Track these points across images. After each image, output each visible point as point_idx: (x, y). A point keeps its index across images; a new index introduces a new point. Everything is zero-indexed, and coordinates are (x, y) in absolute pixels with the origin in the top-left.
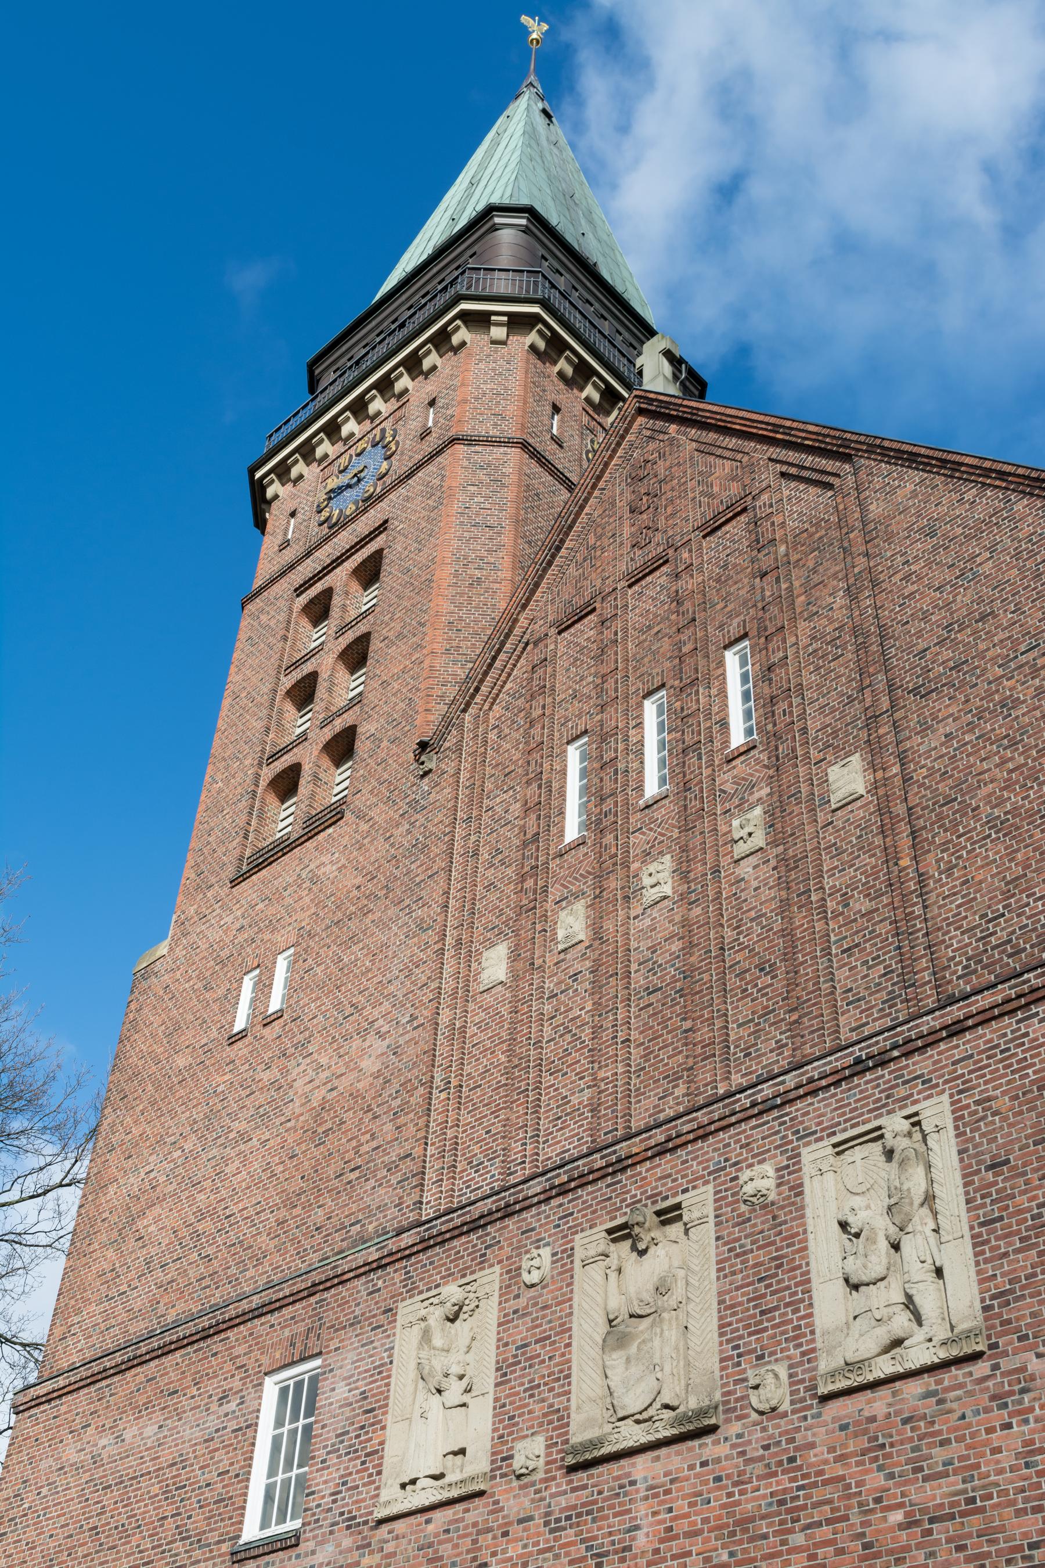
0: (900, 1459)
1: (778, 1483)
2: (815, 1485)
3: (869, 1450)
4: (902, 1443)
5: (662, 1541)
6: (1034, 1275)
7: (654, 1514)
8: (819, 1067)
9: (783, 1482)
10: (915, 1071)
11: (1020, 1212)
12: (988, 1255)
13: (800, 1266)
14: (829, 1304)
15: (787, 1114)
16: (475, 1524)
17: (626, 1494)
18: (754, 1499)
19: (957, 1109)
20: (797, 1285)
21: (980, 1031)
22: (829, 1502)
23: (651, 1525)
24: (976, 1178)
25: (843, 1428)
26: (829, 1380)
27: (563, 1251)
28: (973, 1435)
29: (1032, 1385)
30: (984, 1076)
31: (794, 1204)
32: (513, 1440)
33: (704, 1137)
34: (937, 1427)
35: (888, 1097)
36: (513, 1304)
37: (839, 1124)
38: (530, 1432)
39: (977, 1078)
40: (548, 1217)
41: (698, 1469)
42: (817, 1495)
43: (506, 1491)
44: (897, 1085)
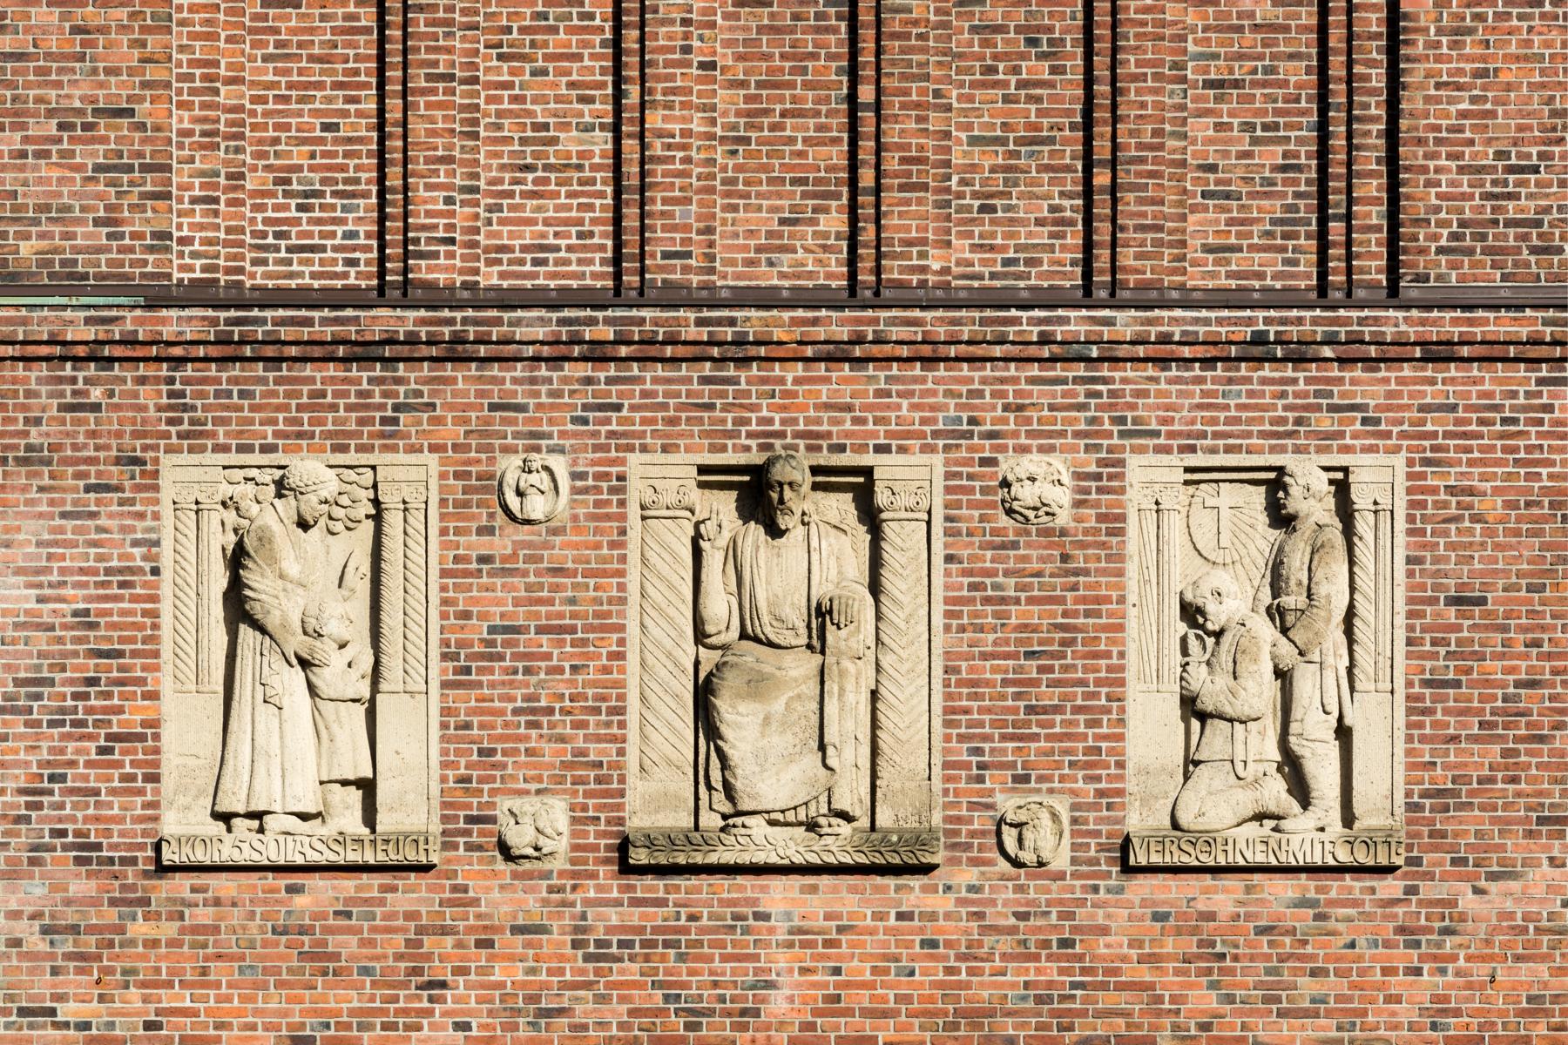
0: (1247, 979)
1: (1038, 971)
2: (1104, 986)
3: (1200, 957)
4: (1252, 958)
5: (817, 1012)
6: (1492, 780)
7: (804, 971)
8: (1184, 321)
10: (1354, 394)
11: (1488, 683)
12: (1428, 731)
13: (1108, 655)
14: (1151, 729)
15: (1105, 381)
16: (409, 916)
17: (747, 931)
20: (1098, 682)
21: (1475, 370)
23: (799, 985)
24: (1429, 609)
25: (1158, 917)
28: (1362, 972)
29: (1460, 927)
30: (1468, 450)
31: (1103, 545)
32: (493, 792)
33: (929, 361)
34: (1309, 950)
35: (1298, 422)
36: (474, 545)
37: (1204, 435)
38: (533, 787)
39: (1458, 449)
40: (557, 394)
41: (892, 921)
42: (1104, 1000)
43: (483, 875)
44: (1318, 408)
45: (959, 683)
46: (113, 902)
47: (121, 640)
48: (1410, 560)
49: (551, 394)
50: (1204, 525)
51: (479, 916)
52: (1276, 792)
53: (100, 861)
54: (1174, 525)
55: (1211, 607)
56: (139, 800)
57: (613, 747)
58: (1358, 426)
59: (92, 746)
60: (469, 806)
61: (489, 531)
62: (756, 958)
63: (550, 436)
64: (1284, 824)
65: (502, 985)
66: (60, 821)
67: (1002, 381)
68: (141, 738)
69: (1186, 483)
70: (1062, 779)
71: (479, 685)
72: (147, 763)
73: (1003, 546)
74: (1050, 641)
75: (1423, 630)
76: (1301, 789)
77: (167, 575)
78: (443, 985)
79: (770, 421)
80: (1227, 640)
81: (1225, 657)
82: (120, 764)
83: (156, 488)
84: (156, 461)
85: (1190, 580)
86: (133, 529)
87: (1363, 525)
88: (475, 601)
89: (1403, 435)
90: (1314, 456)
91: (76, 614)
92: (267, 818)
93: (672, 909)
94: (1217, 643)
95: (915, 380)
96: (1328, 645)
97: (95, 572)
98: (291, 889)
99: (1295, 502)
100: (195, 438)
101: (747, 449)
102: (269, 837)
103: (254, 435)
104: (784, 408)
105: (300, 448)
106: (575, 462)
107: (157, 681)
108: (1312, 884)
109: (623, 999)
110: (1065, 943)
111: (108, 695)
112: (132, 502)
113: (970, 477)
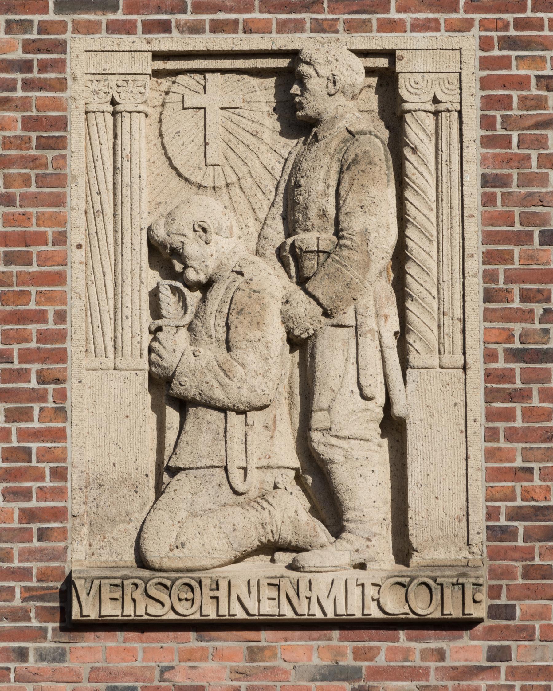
12: (519, 423)
13: (39, 317)
14: (106, 422)
19: (496, 85)
20: (26, 356)
24: (517, 250)
31: (33, 162)
48: (486, 181)
50: (184, 132)
52: (292, 511)
54: (140, 135)
55: (193, 248)
64: (305, 559)
69: (156, 74)
75: (508, 280)
76: (329, 508)
80: (217, 293)
81: (214, 320)
85: (163, 210)
87: (419, 131)
90: (343, 36)
94: (204, 300)
96: (366, 301)
99: (316, 99)
108: (349, 645)
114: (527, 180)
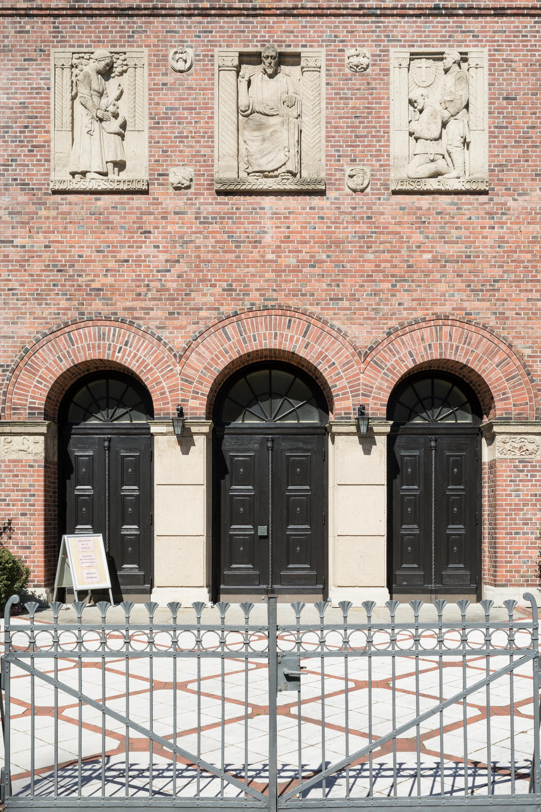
0: (433, 230)
1: (359, 227)
2: (382, 233)
3: (416, 223)
4: (435, 223)
5: (282, 242)
6: (519, 161)
7: (277, 227)
9: (363, 227)
10: (470, 27)
11: (517, 127)
13: (384, 117)
14: (399, 143)
15: (382, 22)
16: (138, 208)
17: (256, 213)
18: (344, 232)
19: (492, 60)
20: (380, 127)
21: (512, 19)
22: (391, 243)
23: (275, 232)
25: (401, 209)
26: (400, 183)
27: (205, 56)
28: (474, 228)
29: (508, 212)
30: (510, 46)
31: (382, 79)
32: (167, 165)
34: (455, 220)
35: (450, 36)
36: (160, 79)
37: (417, 41)
38: (181, 163)
39: (507, 46)
40: (190, 27)
41: (308, 210)
42: (383, 238)
44: (457, 32)
45: (331, 127)
46: (33, 204)
47: (37, 112)
49: (188, 27)
51: (162, 208)
53: (29, 189)
56: (43, 168)
57: (209, 149)
58: (471, 38)
59: (26, 149)
60: (159, 170)
61: (166, 74)
62: (260, 223)
63: (187, 42)
65: (170, 233)
66: (15, 175)
67: (345, 22)
68: (43, 146)
70: (368, 160)
71: (162, 128)
72: (46, 155)
73: (346, 80)
74: (363, 113)
77: (52, 89)
78: (150, 232)
79: (264, 36)
82: (36, 156)
83: (49, 60)
84: (49, 50)
86: (41, 74)
88: (161, 99)
89: (487, 41)
91: (21, 103)
92: (88, 174)
93: (230, 206)
95: (315, 22)
97: (27, 89)
98: (97, 199)
100: (63, 42)
101: (257, 46)
102: (88, 179)
103: (83, 41)
104: (269, 32)
105: (99, 46)
106: (196, 51)
107: (49, 127)
109: (213, 237)
110: (369, 218)
111: (32, 132)
112: (40, 65)
113: (335, 56)
114: (499, 84)
